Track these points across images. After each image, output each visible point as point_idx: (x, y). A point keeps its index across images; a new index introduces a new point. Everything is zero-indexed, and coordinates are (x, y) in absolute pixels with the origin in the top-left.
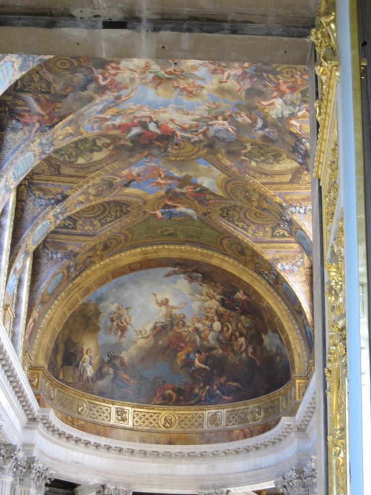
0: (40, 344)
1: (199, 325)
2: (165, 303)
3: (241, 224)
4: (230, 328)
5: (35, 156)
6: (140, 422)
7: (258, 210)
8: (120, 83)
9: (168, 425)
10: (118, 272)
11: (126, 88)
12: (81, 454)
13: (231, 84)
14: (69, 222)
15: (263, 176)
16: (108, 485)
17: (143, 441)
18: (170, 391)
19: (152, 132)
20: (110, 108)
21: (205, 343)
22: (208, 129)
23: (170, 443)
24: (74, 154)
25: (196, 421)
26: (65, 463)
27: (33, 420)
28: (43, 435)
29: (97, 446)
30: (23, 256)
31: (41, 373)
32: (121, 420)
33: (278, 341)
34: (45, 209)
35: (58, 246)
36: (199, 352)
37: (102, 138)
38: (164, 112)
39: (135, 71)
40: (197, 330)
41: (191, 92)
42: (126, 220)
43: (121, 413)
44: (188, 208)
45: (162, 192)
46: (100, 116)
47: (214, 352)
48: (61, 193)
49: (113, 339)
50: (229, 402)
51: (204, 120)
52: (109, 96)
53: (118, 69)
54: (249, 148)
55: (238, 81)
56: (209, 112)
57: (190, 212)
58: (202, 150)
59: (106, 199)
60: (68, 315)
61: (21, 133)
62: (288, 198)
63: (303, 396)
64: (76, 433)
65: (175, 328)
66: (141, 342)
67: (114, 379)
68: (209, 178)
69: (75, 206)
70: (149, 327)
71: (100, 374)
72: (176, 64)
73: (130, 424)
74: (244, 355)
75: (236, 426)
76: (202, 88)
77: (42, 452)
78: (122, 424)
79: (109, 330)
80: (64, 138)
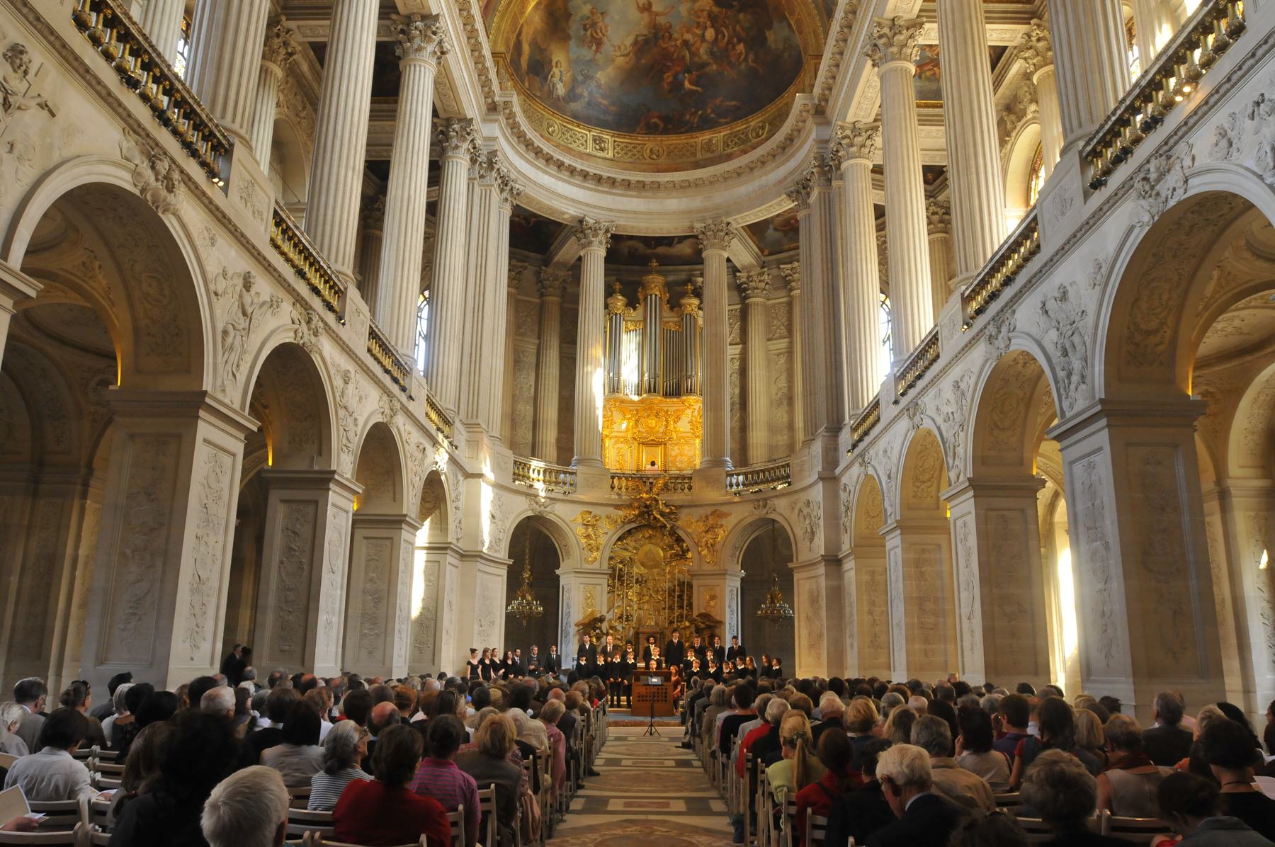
0: (499, 28)
1: (688, 37)
2: (647, 8)
21: (696, 59)
26: (535, 183)
29: (572, 171)
33: (786, 32)
36: (689, 71)
47: (707, 69)
49: (587, 53)
50: (726, 123)
65: (660, 42)
66: (620, 61)
67: (589, 104)
70: (629, 41)
71: (572, 95)
73: (610, 155)
74: (743, 66)
79: (582, 41)
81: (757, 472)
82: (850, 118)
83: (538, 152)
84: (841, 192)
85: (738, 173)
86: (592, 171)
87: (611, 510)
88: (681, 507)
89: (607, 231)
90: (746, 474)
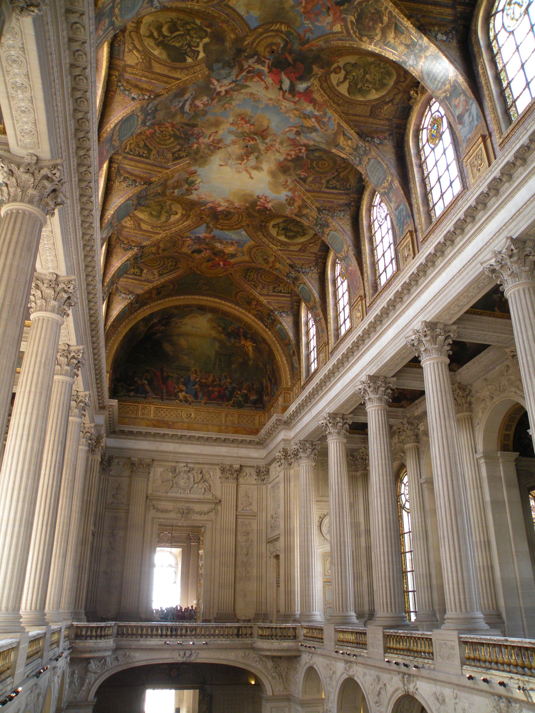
8: (291, 145)
11: (289, 139)
13: (208, 132)
19: (288, 77)
20: (308, 128)
22: (237, 77)
24: (372, 66)
38: (270, 99)
39: (277, 150)
41: (242, 119)
46: (318, 127)
51: (238, 88)
52: (303, 140)
53: (288, 155)
55: (203, 133)
56: (232, 99)
58: (248, 44)
72: (247, 147)
76: (232, 124)
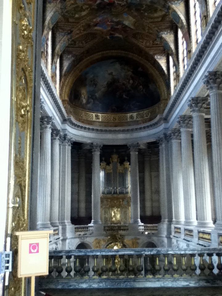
0: (65, 91)
3: (140, 40)
4: (137, 82)
5: (59, 13)
6: (104, 119)
7: (148, 34)
9: (114, 120)
10: (92, 63)
12: (83, 132)
14: (73, 42)
15: (150, 19)
16: (94, 143)
17: (105, 126)
18: (114, 107)
19: (105, 2)
23: (116, 126)
24: (74, 13)
25: (125, 118)
27: (64, 121)
28: (69, 126)
29: (89, 129)
30: (57, 56)
31: (66, 102)
32: (97, 119)
34: (64, 37)
35: (69, 53)
37: (85, 6)
40: (124, 84)
42: (96, 41)
43: (97, 117)
44: (120, 34)
45: (110, 28)
48: (70, 30)
49: (92, 89)
54: (144, 7)
57: (121, 36)
59: (88, 32)
60: (75, 80)
61: (52, 4)
62: (160, 28)
63: (166, 106)
64: (81, 124)
66: (103, 89)
68: (128, 21)
69: (76, 35)
70: (105, 83)
71: (88, 102)
73: (100, 120)
75: (140, 119)
77: (69, 132)
78: (98, 120)
80: (70, 5)
81: (148, 227)
82: (174, 127)
83: (78, 126)
84: (171, 147)
85: (141, 128)
86: (95, 128)
87: (103, 237)
88: (125, 235)
89: (100, 147)
90: (145, 227)
